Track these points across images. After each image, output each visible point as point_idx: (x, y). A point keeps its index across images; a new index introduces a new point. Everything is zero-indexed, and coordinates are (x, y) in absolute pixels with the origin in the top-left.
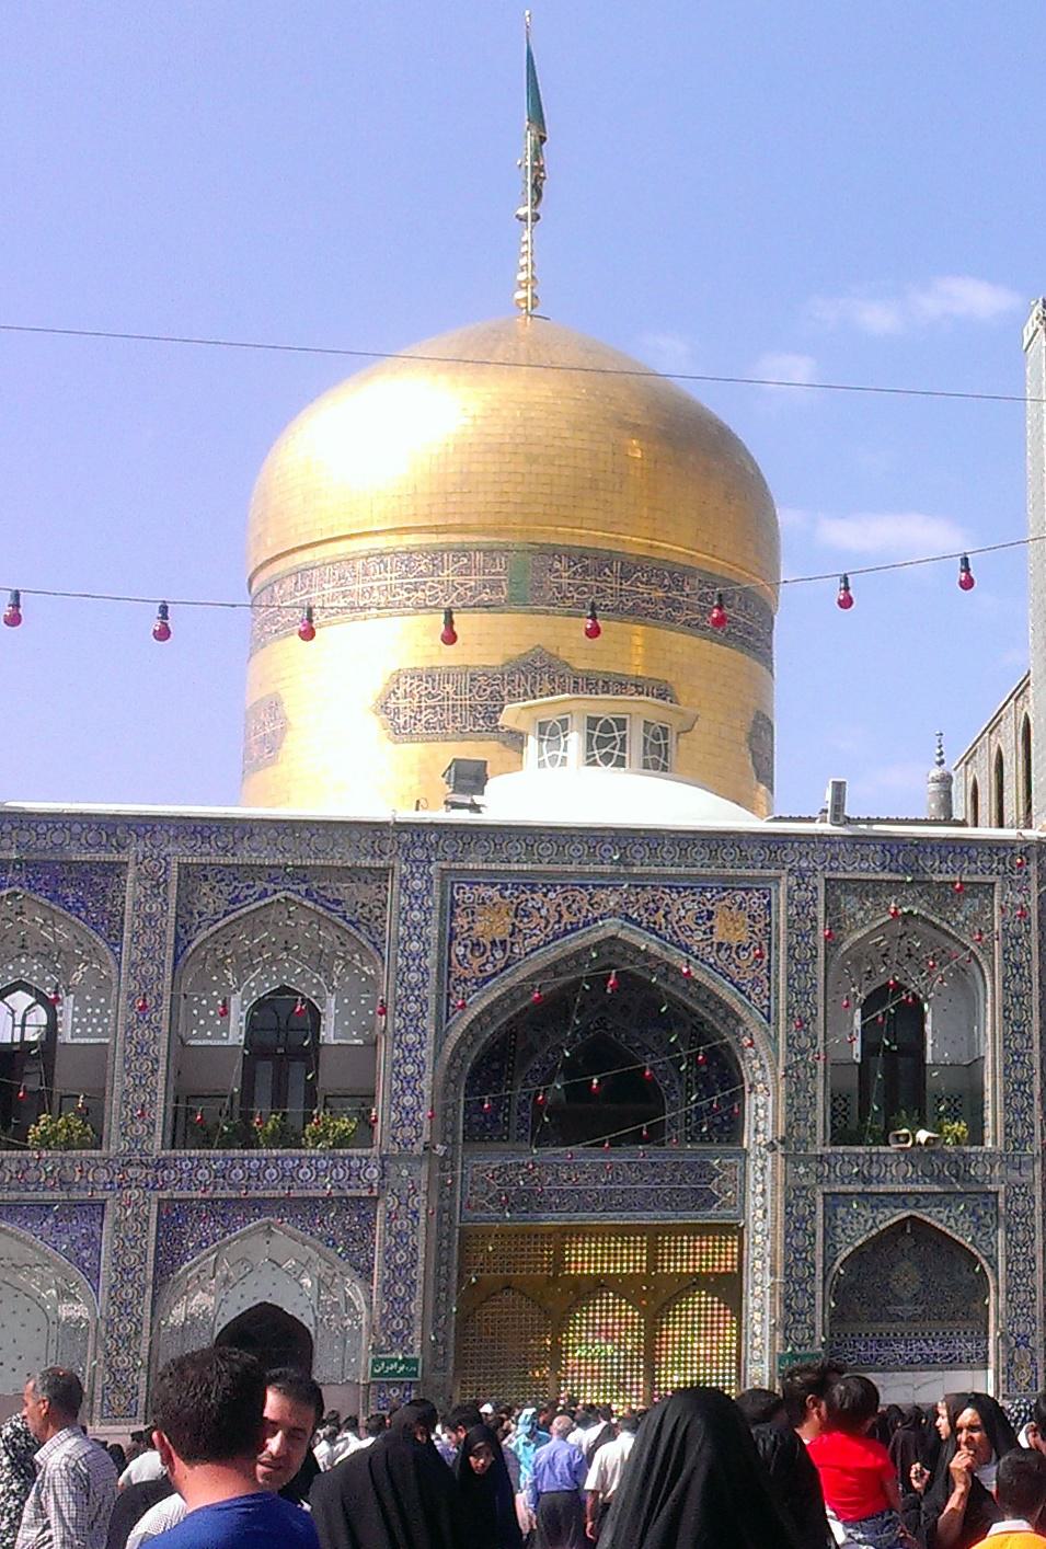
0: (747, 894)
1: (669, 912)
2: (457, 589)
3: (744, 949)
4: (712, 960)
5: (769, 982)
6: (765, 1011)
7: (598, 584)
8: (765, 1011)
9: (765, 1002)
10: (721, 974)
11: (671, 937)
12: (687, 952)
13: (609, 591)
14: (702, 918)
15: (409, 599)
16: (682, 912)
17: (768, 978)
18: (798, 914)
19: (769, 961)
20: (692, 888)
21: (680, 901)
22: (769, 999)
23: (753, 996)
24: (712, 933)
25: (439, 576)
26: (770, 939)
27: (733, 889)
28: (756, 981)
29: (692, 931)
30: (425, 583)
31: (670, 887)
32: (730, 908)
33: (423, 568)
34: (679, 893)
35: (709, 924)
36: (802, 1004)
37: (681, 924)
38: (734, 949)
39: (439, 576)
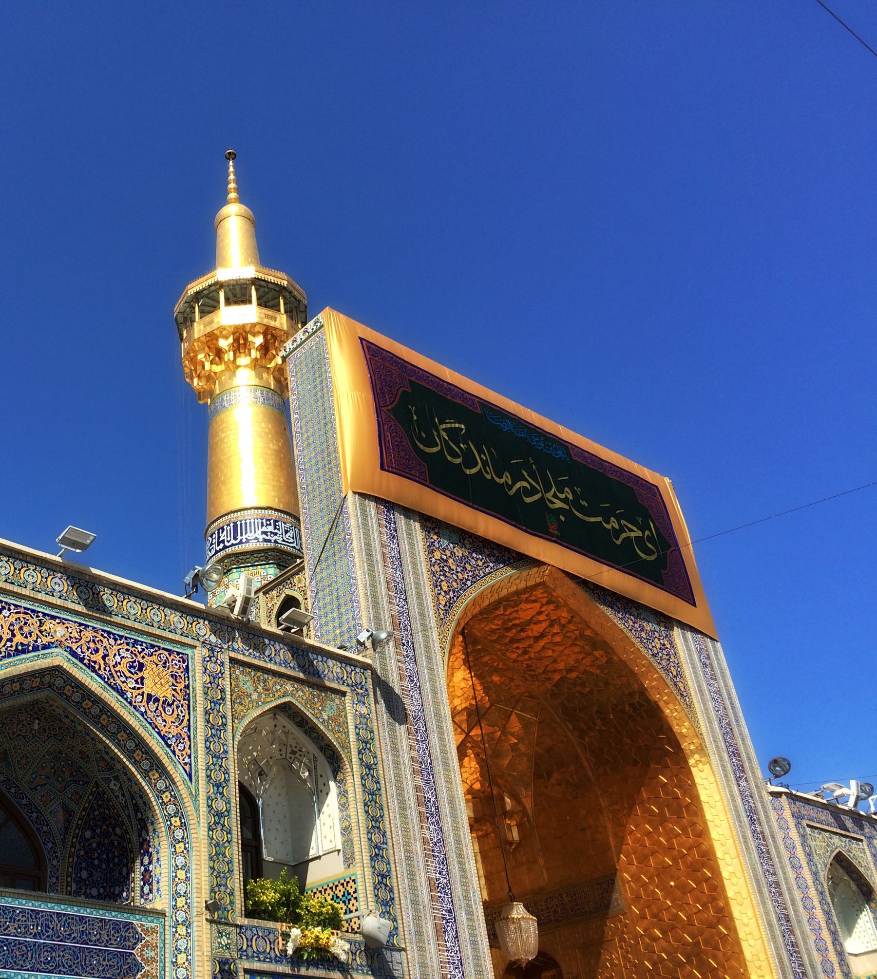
0: (170, 655)
1: (108, 655)
3: (170, 705)
4: (142, 709)
5: (190, 741)
6: (187, 768)
8: (187, 768)
9: (187, 760)
10: (150, 724)
11: (109, 679)
12: (122, 697)
14: (134, 668)
16: (118, 658)
17: (189, 737)
18: (210, 683)
19: (189, 720)
20: (126, 638)
21: (116, 648)
22: (190, 757)
23: (177, 752)
24: (142, 684)
26: (189, 701)
27: (159, 647)
28: (178, 737)
29: (127, 678)
31: (109, 633)
32: (157, 665)
34: (116, 640)
35: (140, 675)
36: (217, 767)
37: (117, 669)
38: (161, 702)
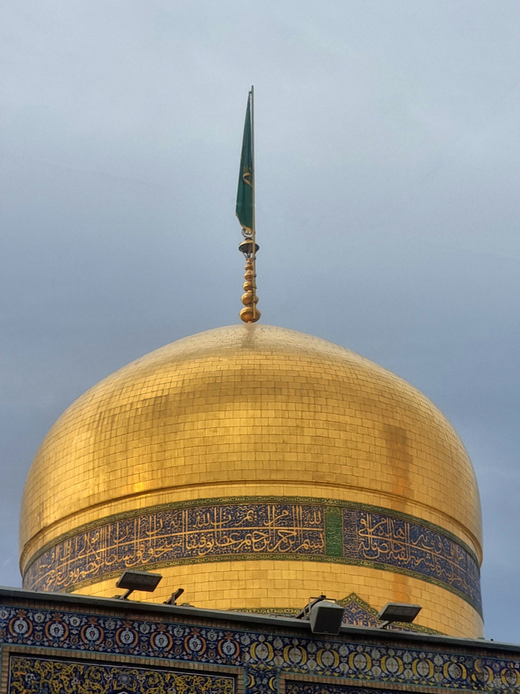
2: (281, 538)
7: (395, 541)
13: (403, 549)
15: (236, 545)
25: (264, 526)
30: (251, 531)
33: (248, 517)
39: (264, 526)
